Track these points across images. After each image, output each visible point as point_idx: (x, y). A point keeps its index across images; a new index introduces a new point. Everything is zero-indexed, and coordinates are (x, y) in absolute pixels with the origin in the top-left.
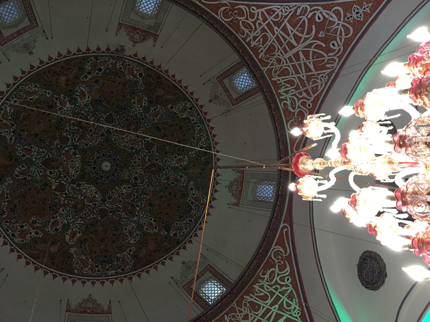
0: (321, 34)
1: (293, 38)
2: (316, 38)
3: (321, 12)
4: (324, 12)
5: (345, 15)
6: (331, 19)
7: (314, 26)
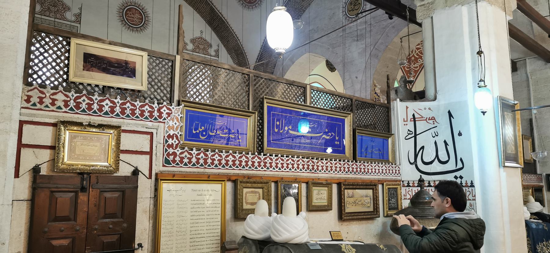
0: (413, 58)
1: (420, 47)
2: (413, 56)
3: (421, 62)
4: (420, 63)
5: (413, 70)
6: (416, 64)
7: (418, 57)
